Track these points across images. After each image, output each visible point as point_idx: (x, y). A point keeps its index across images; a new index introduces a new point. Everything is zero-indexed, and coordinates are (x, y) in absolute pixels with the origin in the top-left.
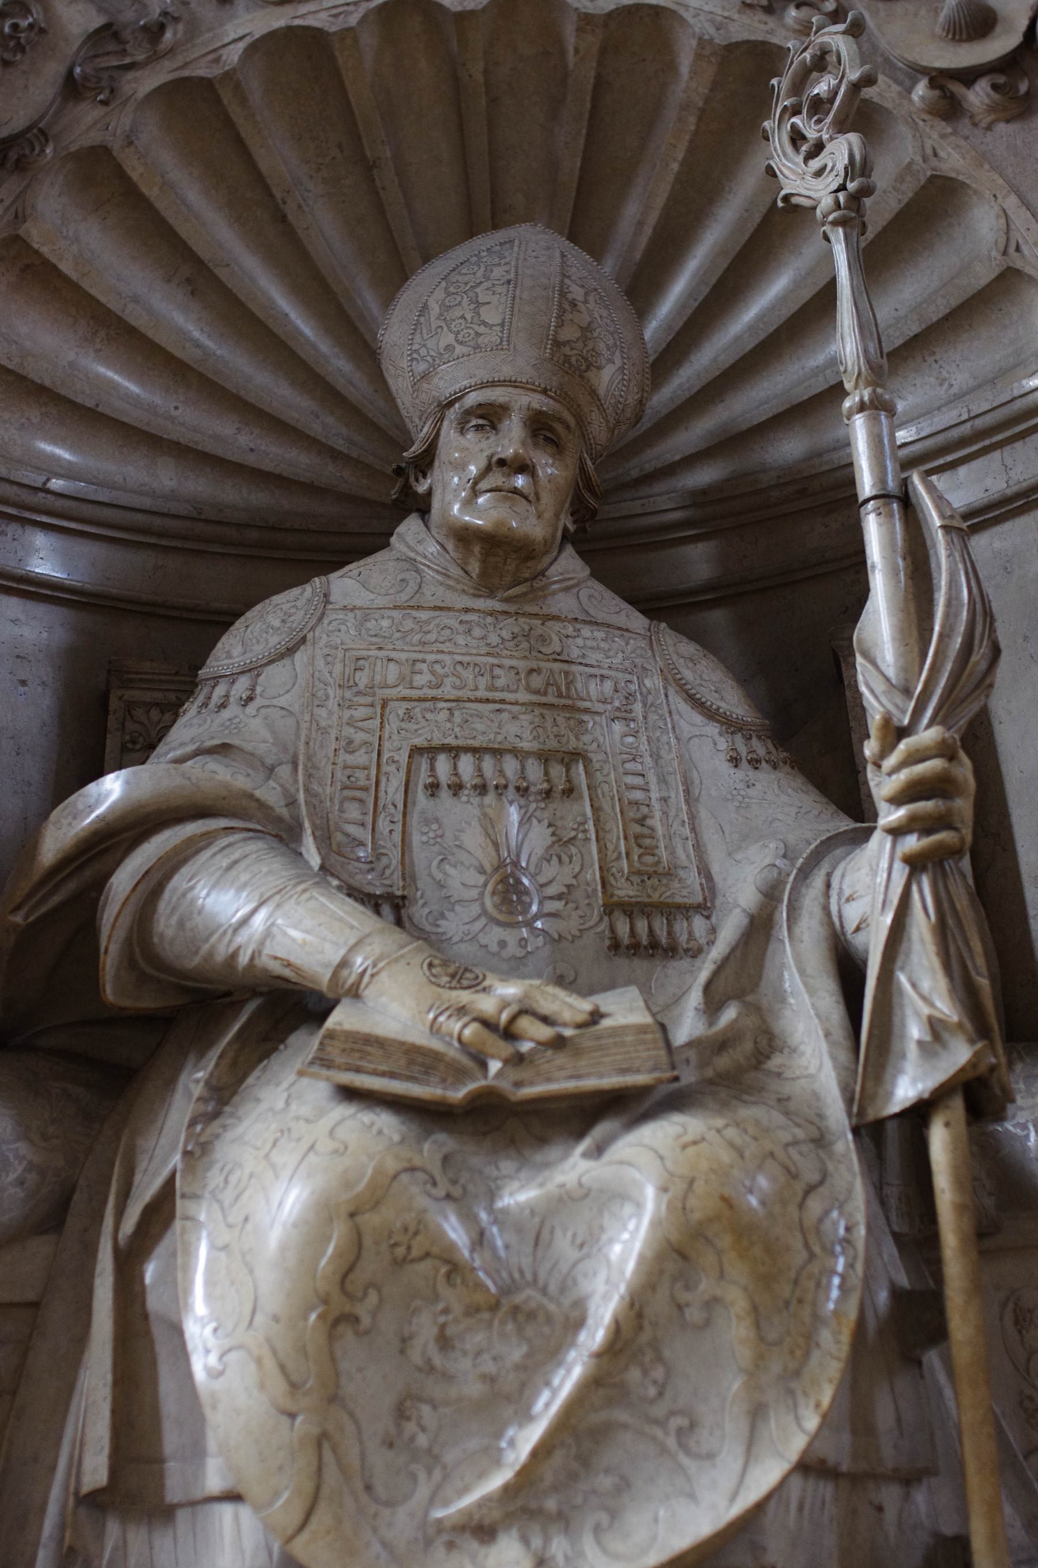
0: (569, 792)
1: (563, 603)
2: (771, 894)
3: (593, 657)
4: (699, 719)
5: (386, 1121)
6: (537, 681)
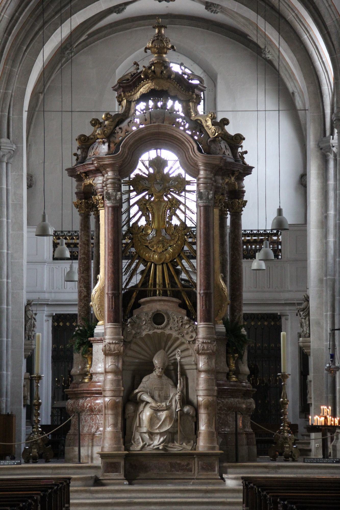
1: (163, 378)
2: (173, 396)
5: (153, 410)
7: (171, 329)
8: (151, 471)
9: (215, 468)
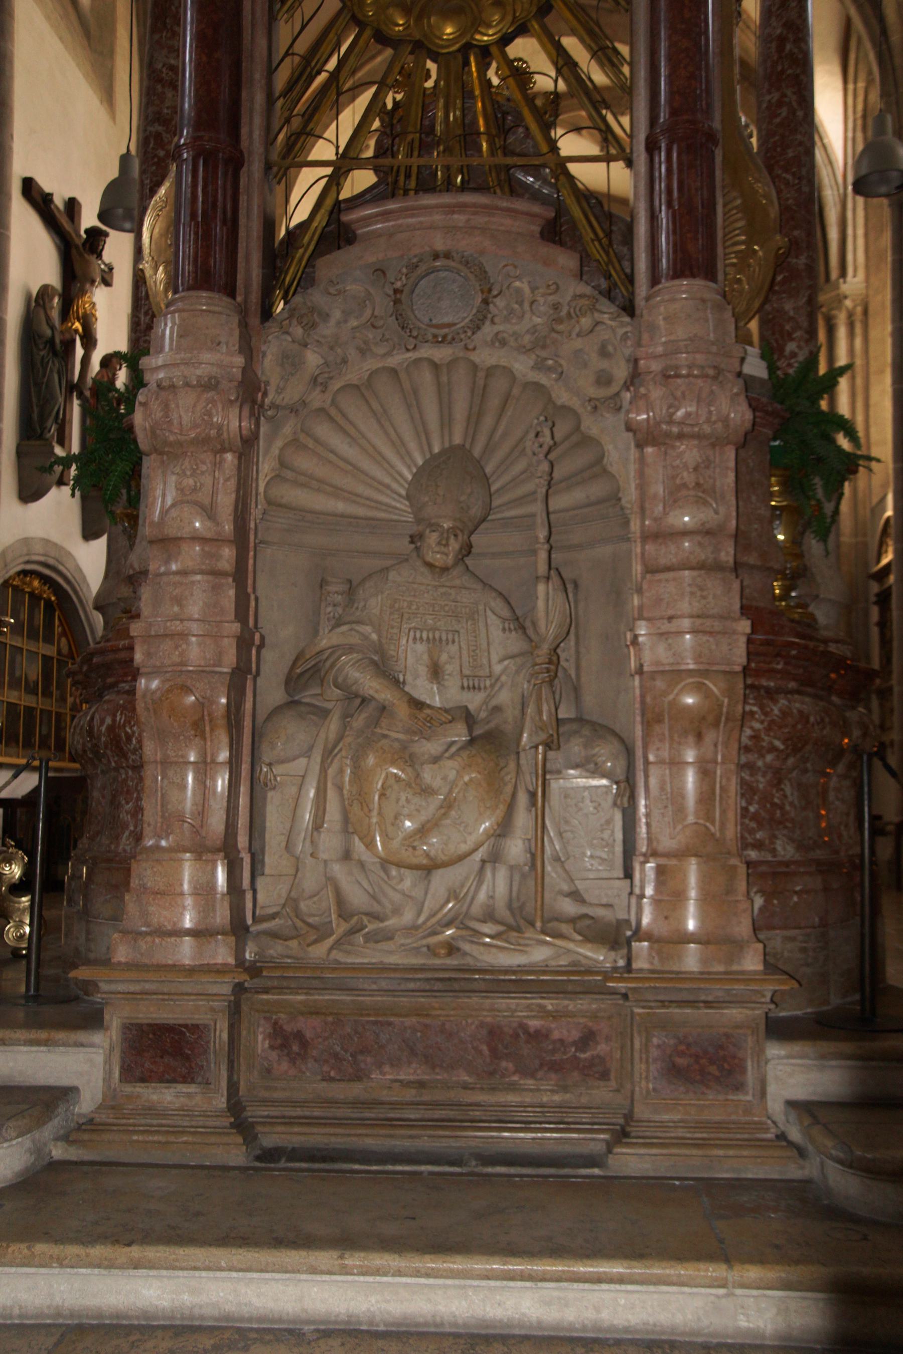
0: (453, 642)
3: (464, 600)
4: (494, 617)
6: (447, 608)
7: (500, 341)
8: (387, 1068)
9: (743, 1071)
